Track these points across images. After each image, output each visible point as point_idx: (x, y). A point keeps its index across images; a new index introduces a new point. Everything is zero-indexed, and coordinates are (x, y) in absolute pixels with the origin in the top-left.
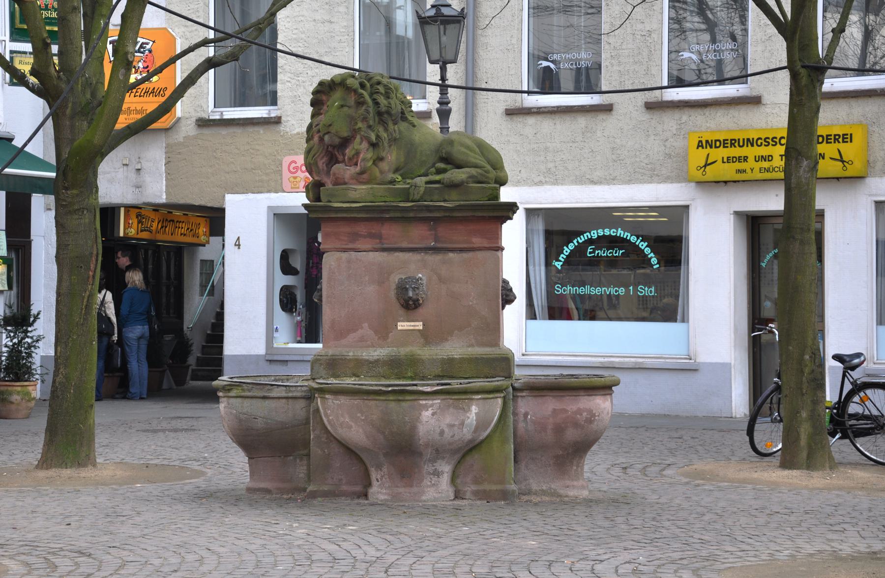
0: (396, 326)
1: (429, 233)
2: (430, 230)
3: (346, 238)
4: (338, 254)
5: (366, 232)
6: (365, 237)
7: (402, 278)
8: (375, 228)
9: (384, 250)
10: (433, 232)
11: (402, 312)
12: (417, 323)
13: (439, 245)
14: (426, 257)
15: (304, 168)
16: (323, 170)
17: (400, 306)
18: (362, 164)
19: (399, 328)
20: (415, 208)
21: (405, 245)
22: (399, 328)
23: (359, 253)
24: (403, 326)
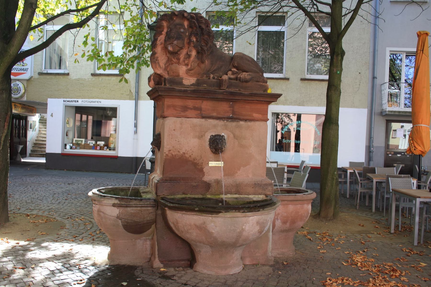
0: (208, 164)
1: (229, 109)
2: (230, 107)
3: (180, 109)
4: (175, 119)
5: (192, 106)
6: (191, 109)
7: (213, 136)
8: (198, 103)
9: (203, 117)
10: (232, 109)
11: (211, 155)
12: (220, 163)
13: (235, 117)
14: (227, 123)
15: (306, 8)
16: (163, 67)
17: (211, 152)
18: (193, 64)
19: (210, 165)
20: (225, 93)
21: (215, 114)
22: (210, 165)
23: (188, 119)
24: (212, 164)
